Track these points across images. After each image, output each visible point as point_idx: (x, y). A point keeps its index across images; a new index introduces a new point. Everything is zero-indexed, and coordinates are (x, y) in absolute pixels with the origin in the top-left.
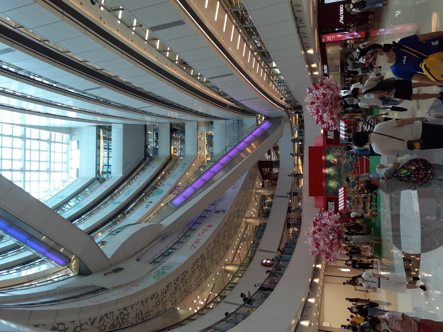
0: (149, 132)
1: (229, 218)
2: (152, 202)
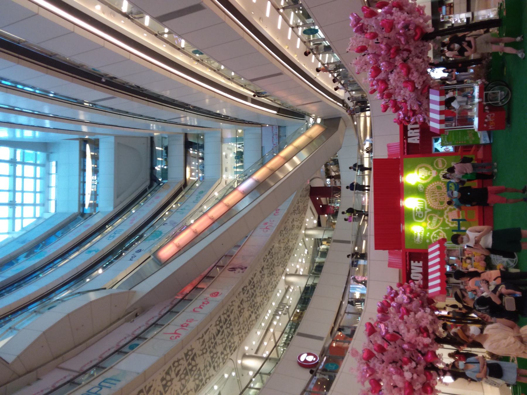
0: (157, 148)
1: (250, 279)
2: (141, 250)
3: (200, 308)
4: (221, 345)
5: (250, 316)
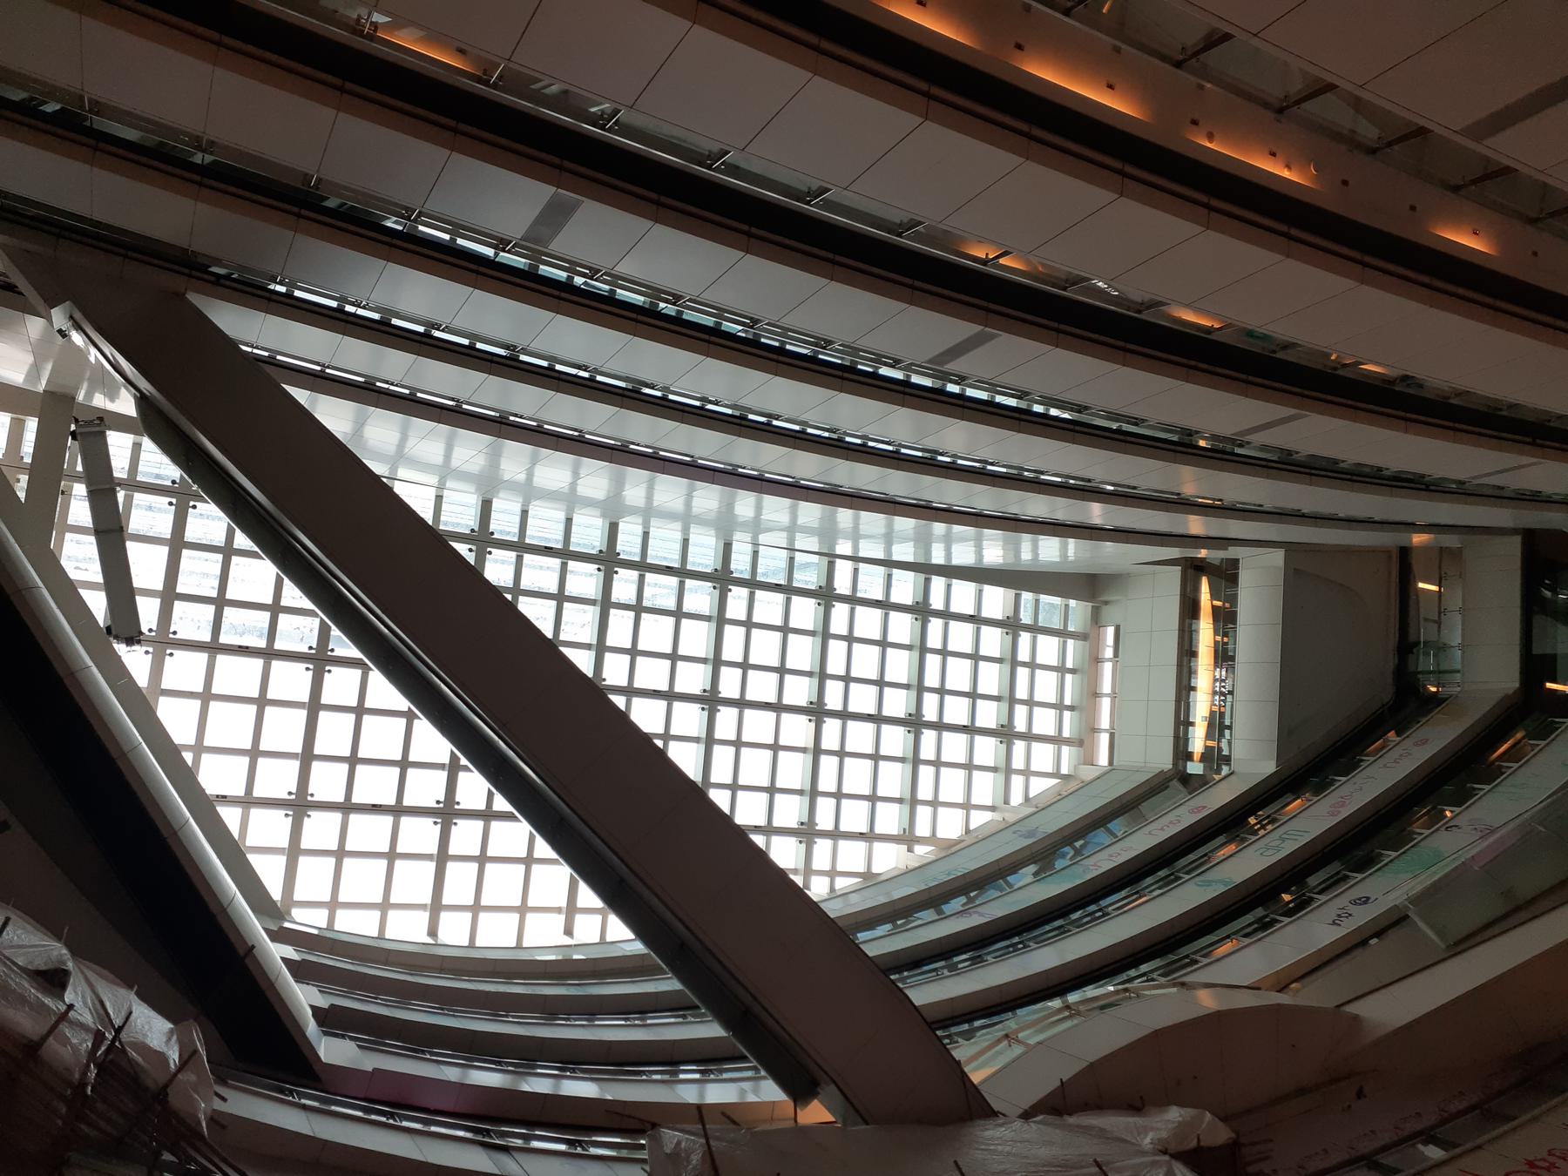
0: (1421, 585)
2: (1368, 898)
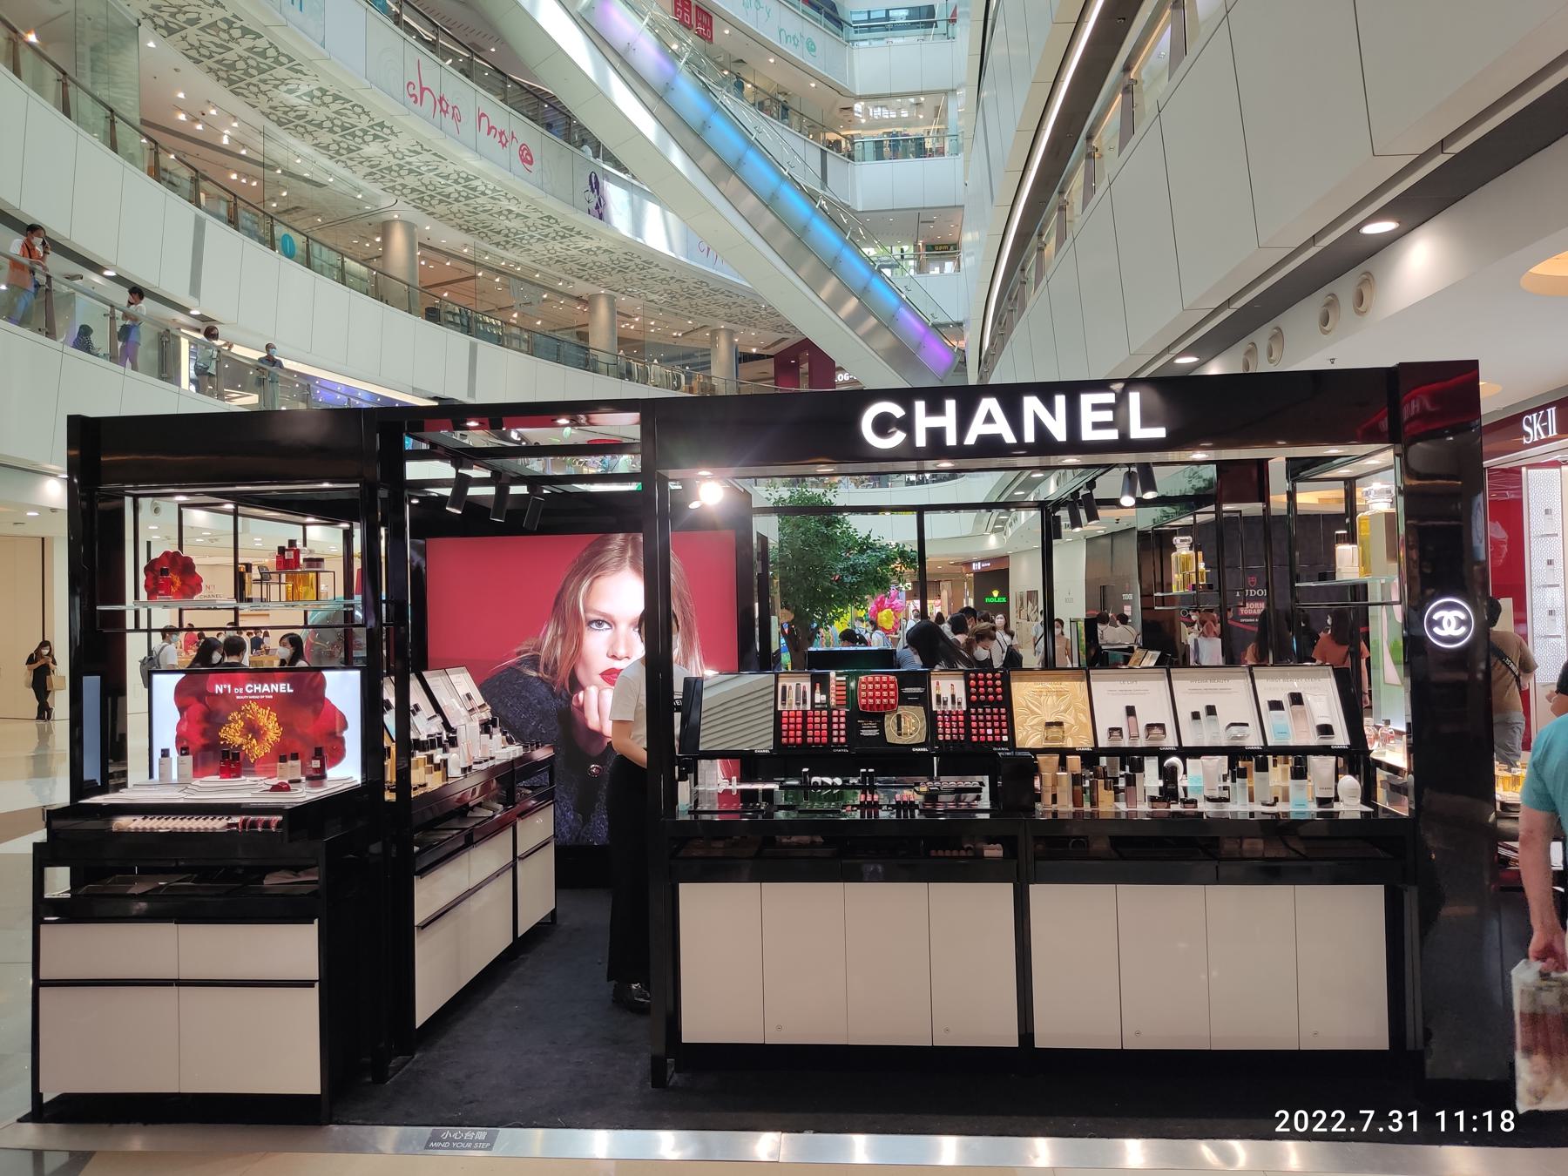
3: (490, 129)
4: (420, 184)
5: (499, 233)
